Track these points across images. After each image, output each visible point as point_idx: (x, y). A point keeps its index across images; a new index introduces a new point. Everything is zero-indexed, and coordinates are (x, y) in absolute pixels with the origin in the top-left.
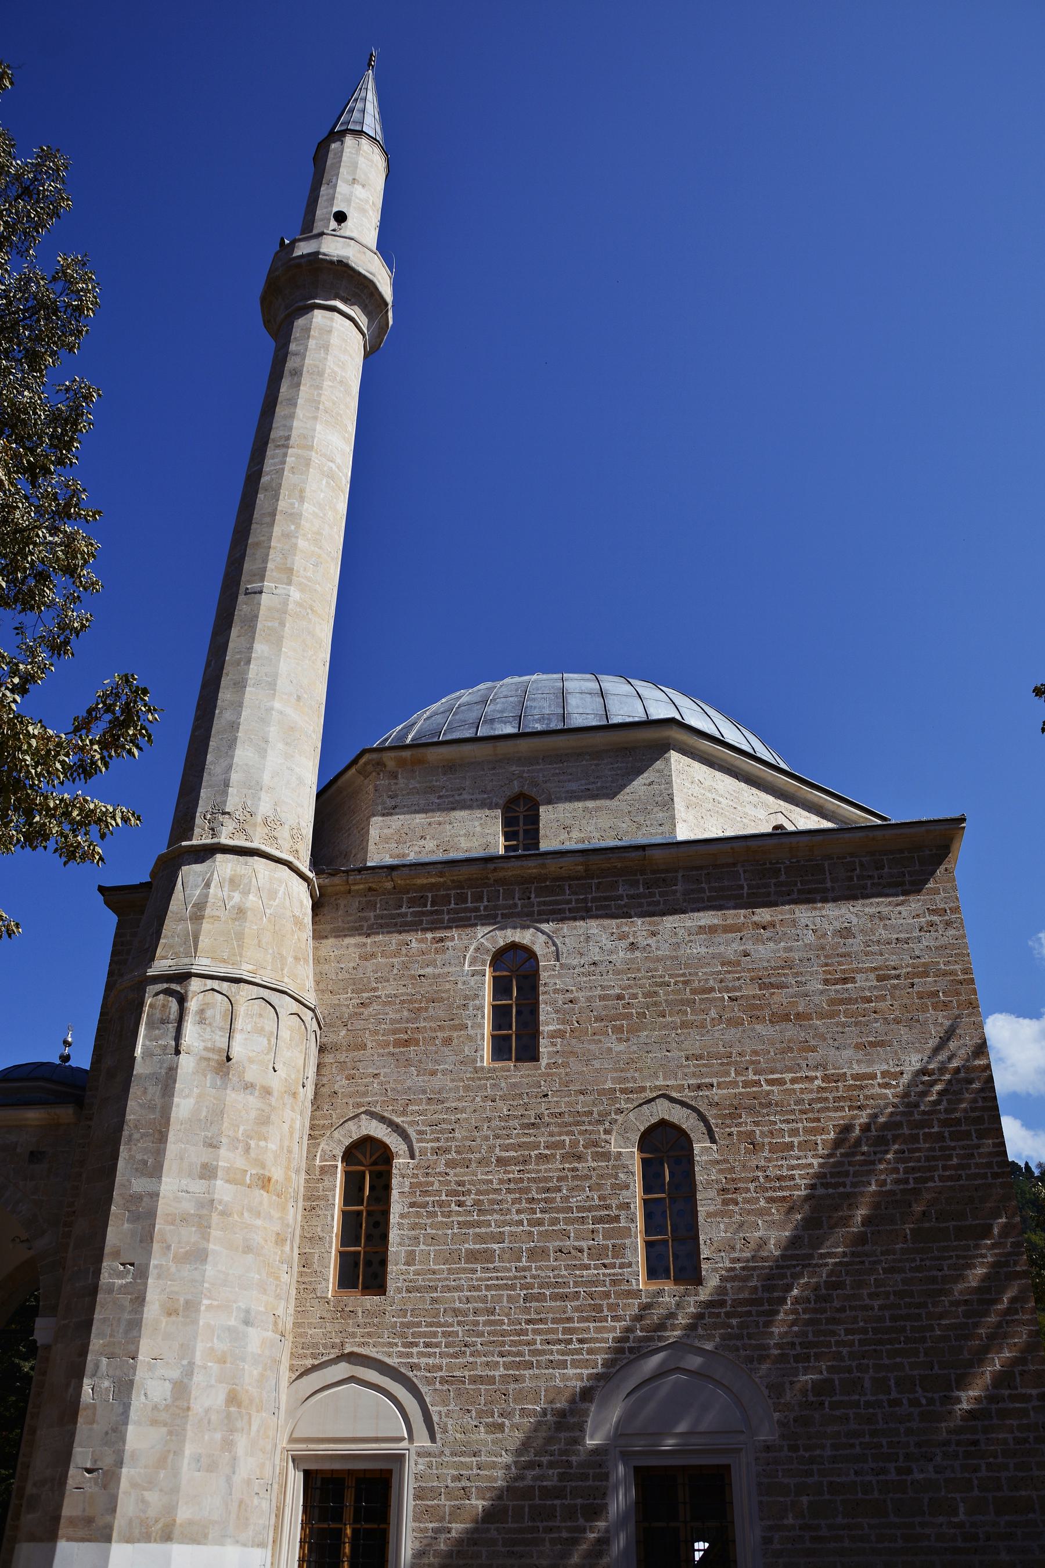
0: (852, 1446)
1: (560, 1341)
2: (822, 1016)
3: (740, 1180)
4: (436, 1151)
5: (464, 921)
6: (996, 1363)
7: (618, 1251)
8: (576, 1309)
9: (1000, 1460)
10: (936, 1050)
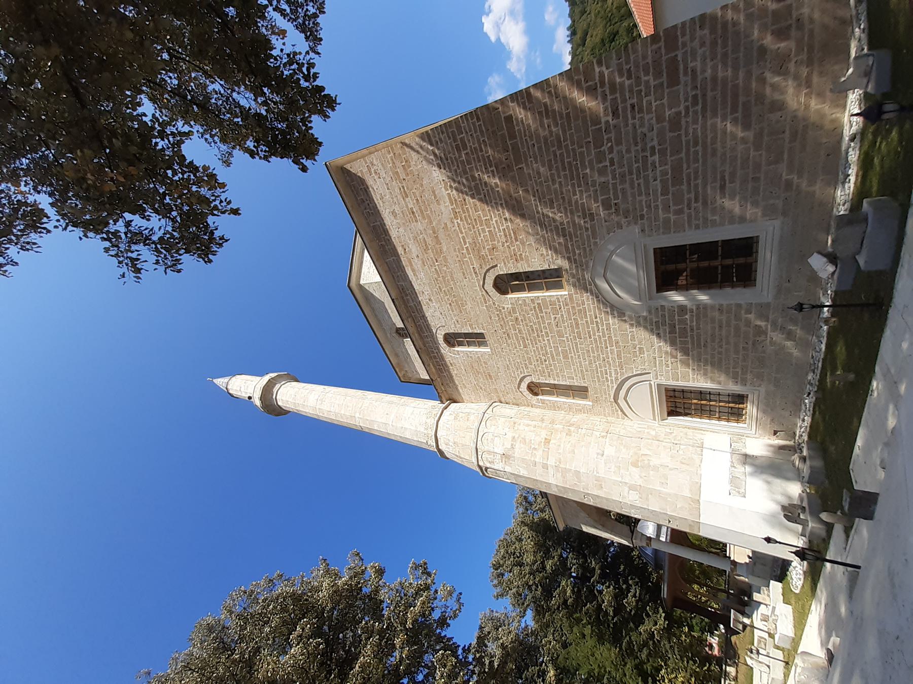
0: (639, 185)
1: (597, 326)
2: (431, 222)
3: (510, 252)
4: (527, 368)
5: (442, 358)
6: (582, 99)
7: (552, 303)
8: (582, 320)
9: (642, 87)
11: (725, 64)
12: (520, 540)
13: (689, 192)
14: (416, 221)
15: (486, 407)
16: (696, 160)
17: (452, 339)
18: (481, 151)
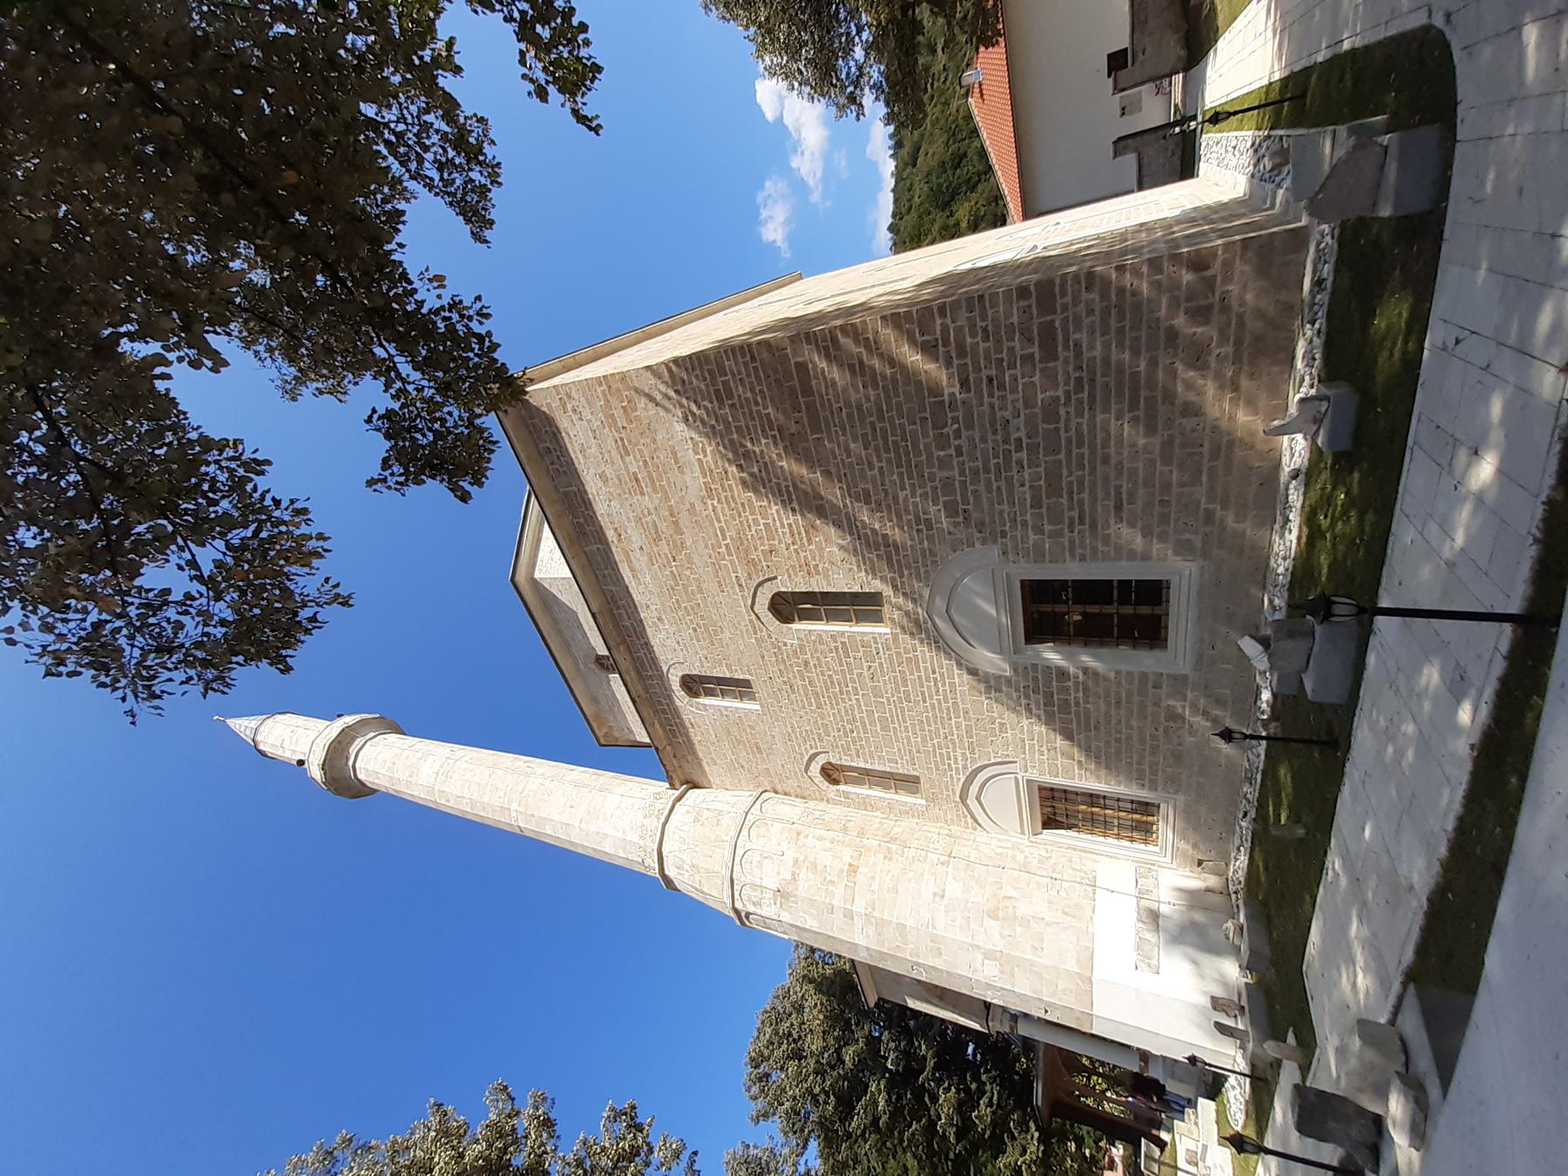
0: (999, 488)
2: (667, 499)
4: (821, 740)
5: (676, 713)
6: (914, 358)
10: (667, 410)
11: (1121, 345)
12: (800, 1009)
13: (1071, 508)
14: (642, 494)
15: (751, 800)
16: (1081, 466)
17: (693, 685)
18: (757, 403)
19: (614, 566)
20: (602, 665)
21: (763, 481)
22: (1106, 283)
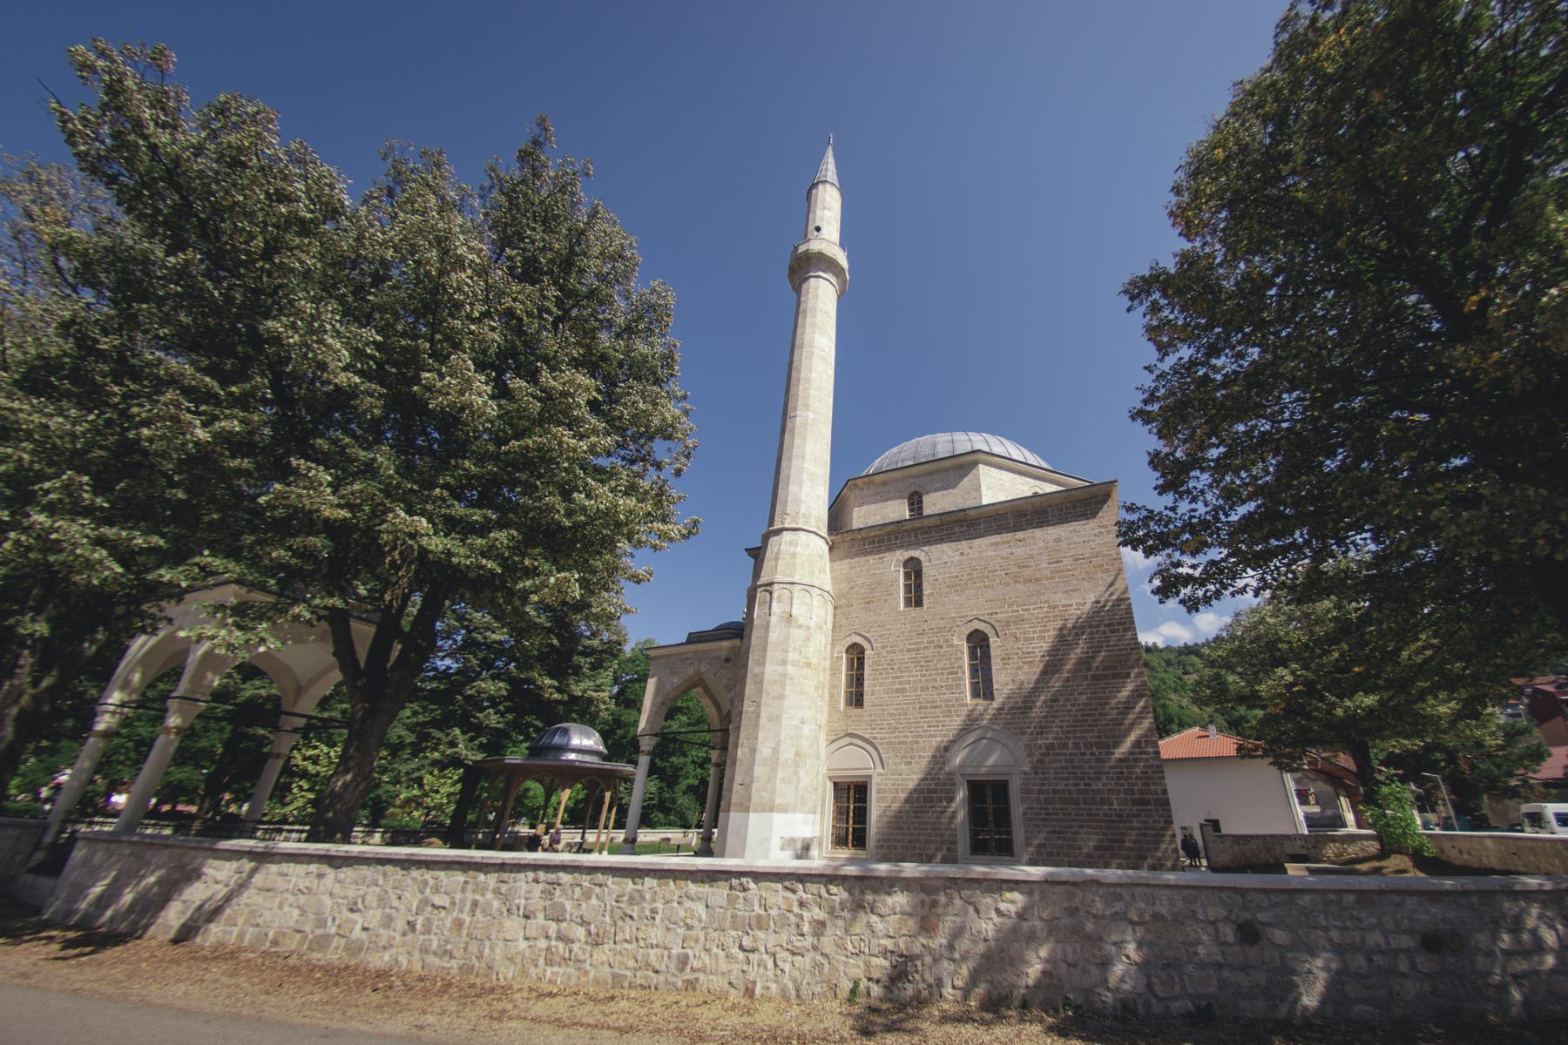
5: (890, 549)
6: (1132, 737)
19: (998, 532)
20: (912, 495)
21: (1063, 641)
22: (1166, 829)
